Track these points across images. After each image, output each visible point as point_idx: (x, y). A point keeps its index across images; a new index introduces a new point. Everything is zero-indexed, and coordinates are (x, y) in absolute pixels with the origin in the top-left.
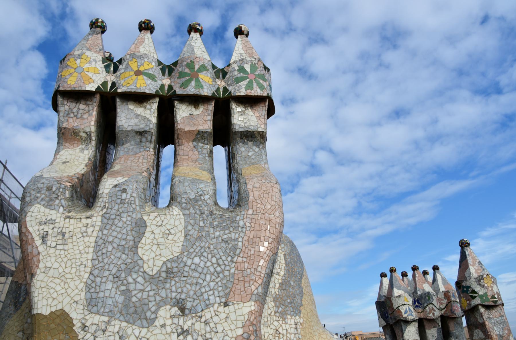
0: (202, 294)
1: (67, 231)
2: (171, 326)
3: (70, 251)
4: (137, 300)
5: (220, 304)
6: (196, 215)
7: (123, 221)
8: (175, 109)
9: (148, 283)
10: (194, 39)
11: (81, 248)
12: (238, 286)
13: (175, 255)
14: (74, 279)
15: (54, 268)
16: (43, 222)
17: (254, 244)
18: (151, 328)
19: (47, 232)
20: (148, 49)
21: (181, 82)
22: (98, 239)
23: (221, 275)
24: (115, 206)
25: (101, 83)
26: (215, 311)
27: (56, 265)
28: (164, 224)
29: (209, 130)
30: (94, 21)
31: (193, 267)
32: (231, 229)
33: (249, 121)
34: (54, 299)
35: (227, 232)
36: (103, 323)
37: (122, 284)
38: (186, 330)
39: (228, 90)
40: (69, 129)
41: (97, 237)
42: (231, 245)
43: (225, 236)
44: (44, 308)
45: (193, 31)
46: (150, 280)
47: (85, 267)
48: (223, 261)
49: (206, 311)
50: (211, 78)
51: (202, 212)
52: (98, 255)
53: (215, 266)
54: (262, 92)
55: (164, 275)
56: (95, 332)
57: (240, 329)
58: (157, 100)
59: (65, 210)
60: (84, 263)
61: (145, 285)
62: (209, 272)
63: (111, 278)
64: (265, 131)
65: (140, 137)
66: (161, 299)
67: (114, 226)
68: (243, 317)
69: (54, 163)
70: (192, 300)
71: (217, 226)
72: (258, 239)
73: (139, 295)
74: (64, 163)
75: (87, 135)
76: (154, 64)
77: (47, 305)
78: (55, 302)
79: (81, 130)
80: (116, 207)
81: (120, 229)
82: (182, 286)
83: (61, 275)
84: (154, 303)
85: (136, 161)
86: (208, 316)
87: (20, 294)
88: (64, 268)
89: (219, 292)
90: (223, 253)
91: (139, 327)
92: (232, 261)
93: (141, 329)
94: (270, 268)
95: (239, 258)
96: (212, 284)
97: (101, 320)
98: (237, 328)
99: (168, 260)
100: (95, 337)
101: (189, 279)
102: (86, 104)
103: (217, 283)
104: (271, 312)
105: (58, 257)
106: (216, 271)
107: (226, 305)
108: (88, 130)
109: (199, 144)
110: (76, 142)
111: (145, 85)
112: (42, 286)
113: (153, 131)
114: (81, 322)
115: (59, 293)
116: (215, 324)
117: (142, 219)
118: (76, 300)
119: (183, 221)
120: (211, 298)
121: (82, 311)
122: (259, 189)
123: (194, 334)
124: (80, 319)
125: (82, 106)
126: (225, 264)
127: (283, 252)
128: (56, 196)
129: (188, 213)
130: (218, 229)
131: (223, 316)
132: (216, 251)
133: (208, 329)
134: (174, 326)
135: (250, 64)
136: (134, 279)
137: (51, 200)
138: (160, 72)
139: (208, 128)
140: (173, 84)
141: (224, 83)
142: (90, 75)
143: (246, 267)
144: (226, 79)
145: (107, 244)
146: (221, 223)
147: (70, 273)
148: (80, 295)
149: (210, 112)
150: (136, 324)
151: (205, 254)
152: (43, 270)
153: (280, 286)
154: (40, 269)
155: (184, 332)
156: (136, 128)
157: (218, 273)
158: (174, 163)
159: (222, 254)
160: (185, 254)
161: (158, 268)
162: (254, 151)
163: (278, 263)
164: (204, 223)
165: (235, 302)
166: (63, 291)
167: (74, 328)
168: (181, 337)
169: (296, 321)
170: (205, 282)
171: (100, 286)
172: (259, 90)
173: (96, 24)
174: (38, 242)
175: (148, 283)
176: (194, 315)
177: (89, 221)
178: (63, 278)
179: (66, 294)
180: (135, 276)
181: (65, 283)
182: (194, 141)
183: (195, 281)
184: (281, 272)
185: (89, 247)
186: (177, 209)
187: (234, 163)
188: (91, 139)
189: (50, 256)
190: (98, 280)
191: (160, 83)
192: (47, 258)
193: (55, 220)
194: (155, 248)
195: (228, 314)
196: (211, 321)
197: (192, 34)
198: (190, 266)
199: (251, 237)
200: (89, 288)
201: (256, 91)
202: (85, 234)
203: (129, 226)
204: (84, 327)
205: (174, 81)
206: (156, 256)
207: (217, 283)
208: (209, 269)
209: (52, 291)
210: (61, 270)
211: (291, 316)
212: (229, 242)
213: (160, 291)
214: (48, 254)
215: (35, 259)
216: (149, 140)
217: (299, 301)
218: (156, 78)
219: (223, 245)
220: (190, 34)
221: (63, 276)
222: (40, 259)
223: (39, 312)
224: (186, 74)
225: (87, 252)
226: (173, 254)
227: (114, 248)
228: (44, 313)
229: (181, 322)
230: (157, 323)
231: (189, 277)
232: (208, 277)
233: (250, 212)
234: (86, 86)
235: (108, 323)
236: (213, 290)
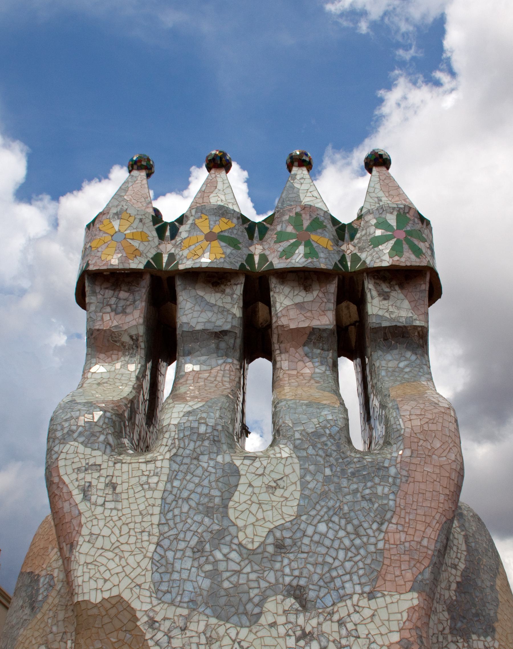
0: (333, 579)
1: (119, 482)
2: (286, 626)
3: (125, 511)
4: (231, 586)
5: (361, 594)
6: (319, 458)
7: (203, 467)
8: (272, 294)
9: (247, 562)
10: (298, 177)
11: (142, 507)
12: (391, 569)
13: (287, 520)
14: (134, 553)
15: (103, 536)
16: (84, 468)
17: (415, 503)
18: (254, 629)
19: (90, 482)
20: (223, 198)
21: (281, 249)
22: (166, 494)
23: (362, 551)
24: (189, 444)
26: (354, 606)
27: (106, 532)
28: (267, 471)
29: (331, 327)
30: (135, 159)
31: (316, 538)
32: (377, 480)
34: (106, 581)
35: (369, 484)
36: (181, 618)
37: (207, 562)
38: (310, 632)
39: (360, 259)
40: (105, 331)
41: (164, 491)
42: (376, 505)
43: (367, 491)
44: (93, 593)
45: (296, 164)
46: (250, 557)
47: (149, 535)
48: (365, 530)
49: (340, 605)
51: (328, 453)
52: (168, 518)
53: (352, 537)
54: (418, 260)
55: (271, 549)
56: (169, 630)
57: (395, 633)
58: (242, 280)
59: (113, 451)
60: (147, 530)
61: (243, 564)
62: (342, 546)
63: (189, 553)
64: (426, 326)
65: (217, 341)
66: (267, 585)
67: (189, 474)
68: (399, 616)
69: (85, 385)
70: (316, 588)
71: (353, 474)
72: (420, 495)
73: (234, 579)
74: (99, 384)
75: (133, 339)
77: (97, 589)
78: (108, 585)
80: (192, 446)
81: (198, 479)
82: (301, 566)
83: (115, 546)
84: (256, 591)
85: (213, 379)
86: (343, 613)
87: (38, 590)
88: (118, 535)
89: (360, 577)
90: (365, 516)
91: (236, 626)
92: (379, 530)
93: (239, 629)
94: (442, 542)
95: (391, 525)
96: (348, 565)
97: (178, 613)
98: (391, 632)
99: (276, 527)
100: (170, 638)
101: (311, 557)
102: (129, 291)
103: (356, 563)
104: (444, 629)
105: (108, 519)
106: (353, 545)
107: (371, 596)
108: (133, 332)
109: (315, 350)
110: (115, 352)
111: (223, 256)
112: (88, 561)
113: (237, 331)
114: (148, 616)
115: (113, 572)
116: (355, 625)
117: (232, 464)
118: (139, 583)
119: (297, 467)
120: (348, 585)
121: (148, 600)
122: (421, 417)
123: (322, 638)
124: (146, 611)
125: (123, 294)
126: (368, 535)
127: (462, 531)
128: (101, 429)
129: (305, 454)
130: (355, 480)
131: (367, 613)
132: (352, 514)
133: (344, 632)
134: (290, 626)
135: (395, 213)
136: (225, 555)
137: (93, 435)
138: (246, 234)
139: (328, 323)
140: (267, 253)
141: (351, 247)
142: (136, 244)
143: (403, 540)
144: (356, 241)
145: (180, 501)
146: (358, 471)
147: (127, 543)
148: (145, 575)
150: (231, 620)
151: (336, 519)
152: (87, 538)
153: (458, 587)
154: (82, 536)
155: (305, 636)
156: (209, 327)
157: (358, 548)
158: (274, 382)
159: (363, 519)
160: (304, 518)
161: (262, 539)
162: (407, 359)
164: (331, 470)
165: (386, 593)
166: (119, 569)
167: (138, 623)
168: (302, 643)
169: (487, 645)
170: (336, 561)
171: (173, 564)
172: (413, 257)
173: (139, 164)
174: (78, 497)
175: (247, 562)
176: (320, 611)
177: (151, 466)
178: (117, 551)
179: (123, 574)
180: (226, 550)
181: (121, 558)
182: (304, 345)
183: (320, 559)
184: (460, 564)
185: (154, 505)
186: (287, 450)
187: (375, 381)
189: (96, 518)
190: (170, 555)
191: (245, 252)
192: (92, 521)
193: (100, 465)
194: (254, 508)
195: (376, 610)
196: (348, 620)
197: (295, 170)
198: (312, 537)
199: (410, 492)
200: (156, 565)
201: (408, 259)
202: (146, 487)
203: (213, 476)
204: (152, 623)
205: (269, 248)
206: (257, 520)
207: (356, 563)
208: (342, 542)
209: (102, 569)
210: (113, 539)
211: (479, 636)
212: (373, 500)
213: (266, 573)
214: (93, 515)
215: (75, 522)
216: (231, 345)
218: (240, 243)
219: (364, 504)
220: (290, 171)
221: (118, 547)
222: (83, 522)
223: (86, 598)
224: (289, 236)
225: (150, 512)
226: (283, 519)
227: (191, 507)
228: (93, 600)
229: (301, 620)
230: (262, 620)
231: (311, 554)
232: (341, 555)
234: (131, 261)
235: (188, 618)
236: (349, 573)
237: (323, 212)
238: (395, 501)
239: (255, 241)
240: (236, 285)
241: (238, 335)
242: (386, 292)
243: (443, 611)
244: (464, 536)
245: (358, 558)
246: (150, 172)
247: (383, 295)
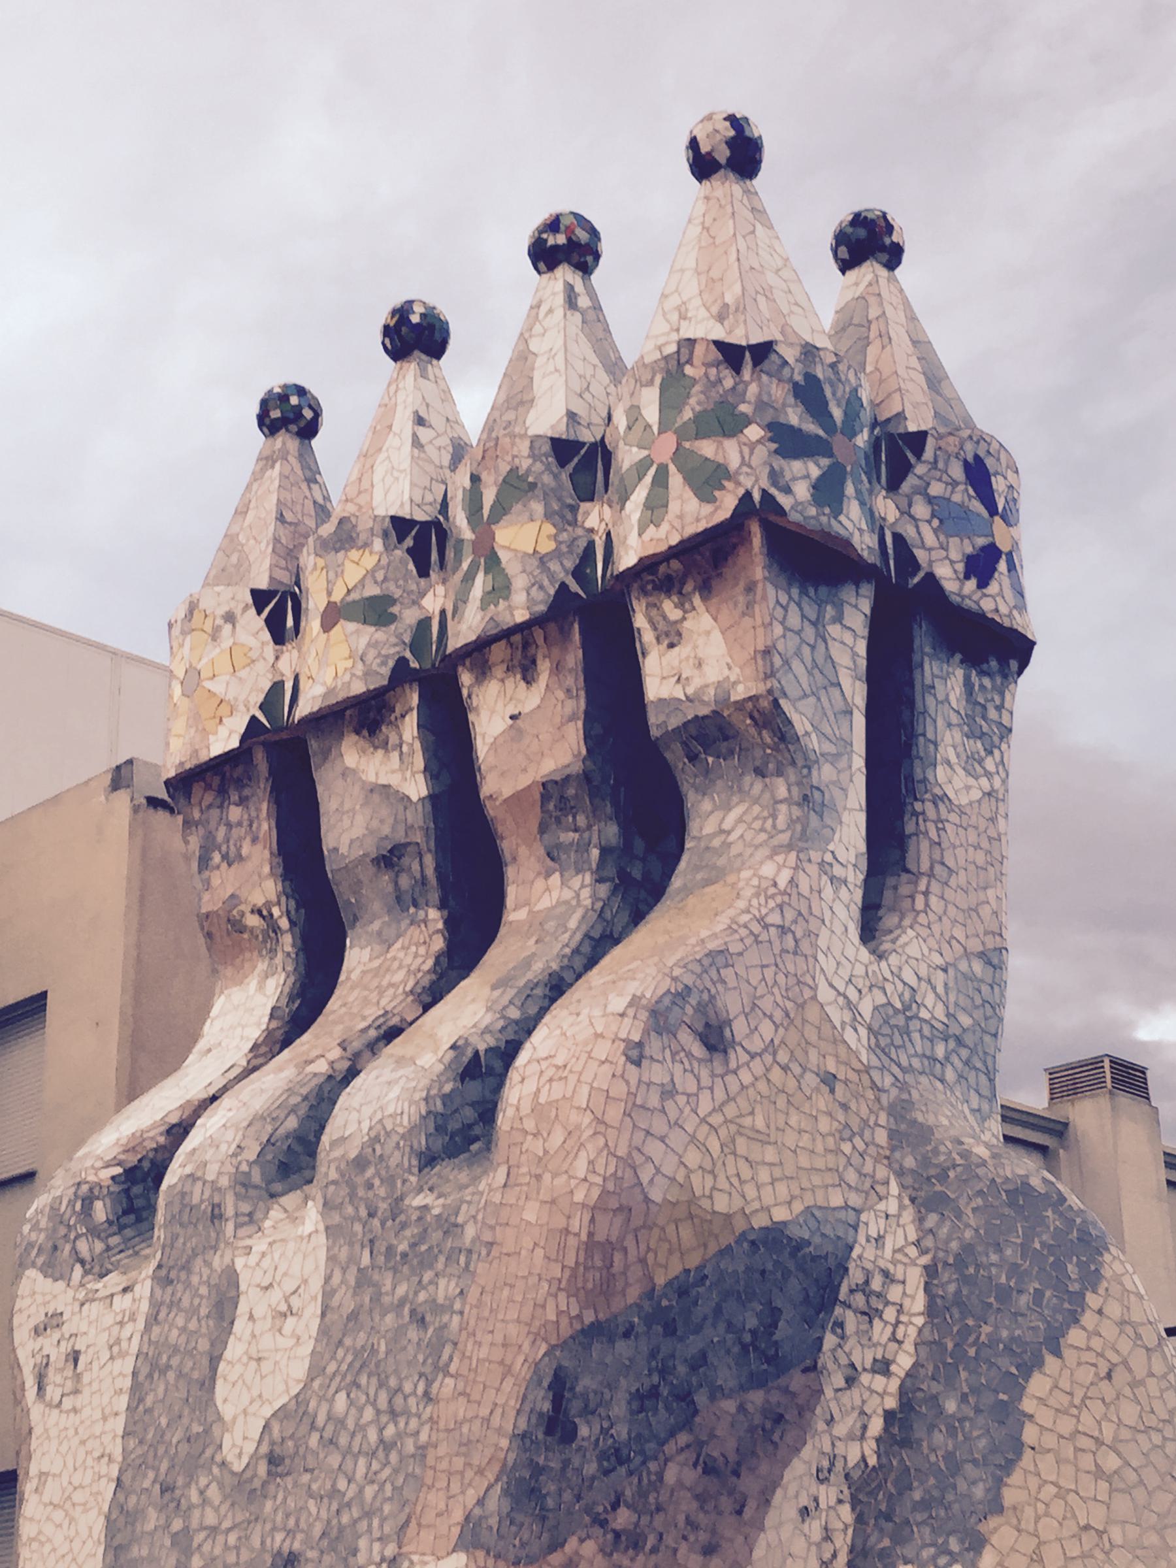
23: (394, 1457)
25: (261, 698)
33: (699, 665)
43: (422, 1296)
50: (548, 516)
54: (707, 509)
55: (262, 1469)
59: (86, 1273)
62: (365, 1447)
76: (378, 545)
79: (242, 907)
108: (259, 900)
113: (418, 837)
119: (322, 1255)
127: (923, 1252)
138: (411, 566)
149: (570, 681)
151: (363, 1380)
160: (316, 1384)
163: (890, 1314)
188: (276, 929)
191: (410, 617)
216: (418, 876)
217: (979, 1492)
221: (69, 1497)
233: (500, 1175)
237: (527, 443)
238: (461, 1313)
239: (434, 575)
240: (403, 716)
241: (424, 846)
242: (676, 622)
243: (840, 1501)
244: (925, 1267)
245: (387, 1472)
246: (302, 424)
247: (667, 635)
